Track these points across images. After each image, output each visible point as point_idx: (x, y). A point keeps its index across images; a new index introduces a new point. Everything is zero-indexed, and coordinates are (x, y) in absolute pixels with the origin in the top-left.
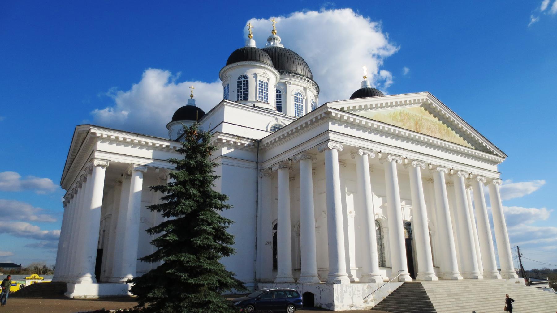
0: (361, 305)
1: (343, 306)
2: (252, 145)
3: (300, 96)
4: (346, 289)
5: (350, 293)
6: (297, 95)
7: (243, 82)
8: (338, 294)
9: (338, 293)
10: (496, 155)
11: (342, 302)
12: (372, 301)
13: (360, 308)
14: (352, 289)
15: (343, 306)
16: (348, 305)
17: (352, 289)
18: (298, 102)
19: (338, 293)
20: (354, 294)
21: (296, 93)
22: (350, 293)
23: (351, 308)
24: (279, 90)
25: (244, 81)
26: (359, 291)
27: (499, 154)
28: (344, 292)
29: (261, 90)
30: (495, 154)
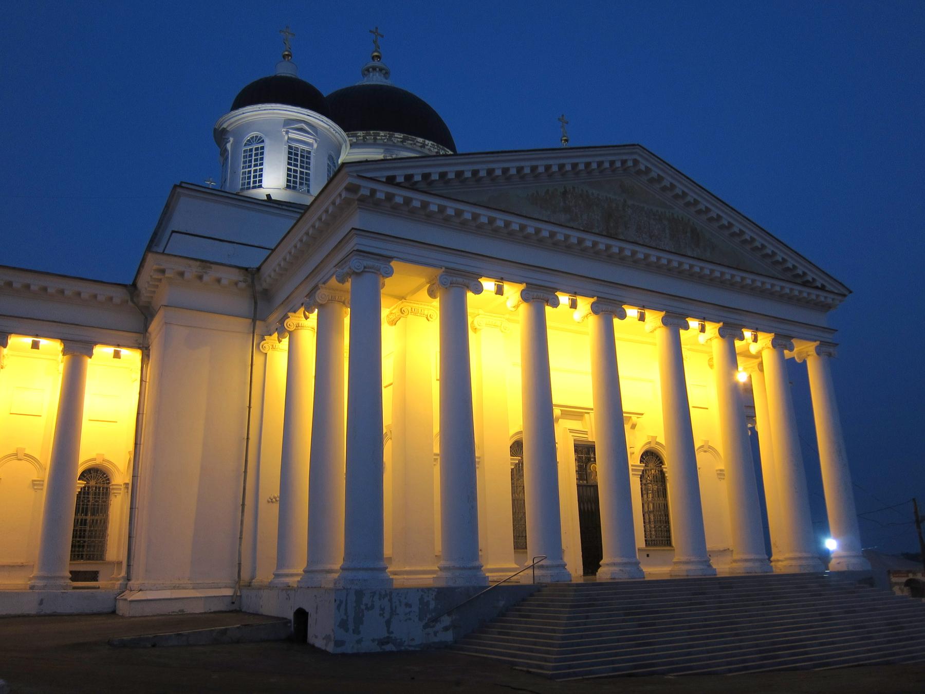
0: (413, 640)
1: (359, 642)
2: (240, 281)
4: (373, 601)
5: (383, 609)
7: (254, 150)
8: (346, 613)
9: (346, 610)
10: (823, 288)
11: (356, 631)
12: (446, 629)
13: (410, 646)
14: (390, 600)
15: (359, 642)
16: (373, 640)
17: (390, 600)
19: (346, 610)
20: (393, 612)
22: (383, 609)
23: (383, 647)
25: (257, 149)
26: (408, 605)
27: (829, 287)
28: (363, 607)
30: (820, 286)
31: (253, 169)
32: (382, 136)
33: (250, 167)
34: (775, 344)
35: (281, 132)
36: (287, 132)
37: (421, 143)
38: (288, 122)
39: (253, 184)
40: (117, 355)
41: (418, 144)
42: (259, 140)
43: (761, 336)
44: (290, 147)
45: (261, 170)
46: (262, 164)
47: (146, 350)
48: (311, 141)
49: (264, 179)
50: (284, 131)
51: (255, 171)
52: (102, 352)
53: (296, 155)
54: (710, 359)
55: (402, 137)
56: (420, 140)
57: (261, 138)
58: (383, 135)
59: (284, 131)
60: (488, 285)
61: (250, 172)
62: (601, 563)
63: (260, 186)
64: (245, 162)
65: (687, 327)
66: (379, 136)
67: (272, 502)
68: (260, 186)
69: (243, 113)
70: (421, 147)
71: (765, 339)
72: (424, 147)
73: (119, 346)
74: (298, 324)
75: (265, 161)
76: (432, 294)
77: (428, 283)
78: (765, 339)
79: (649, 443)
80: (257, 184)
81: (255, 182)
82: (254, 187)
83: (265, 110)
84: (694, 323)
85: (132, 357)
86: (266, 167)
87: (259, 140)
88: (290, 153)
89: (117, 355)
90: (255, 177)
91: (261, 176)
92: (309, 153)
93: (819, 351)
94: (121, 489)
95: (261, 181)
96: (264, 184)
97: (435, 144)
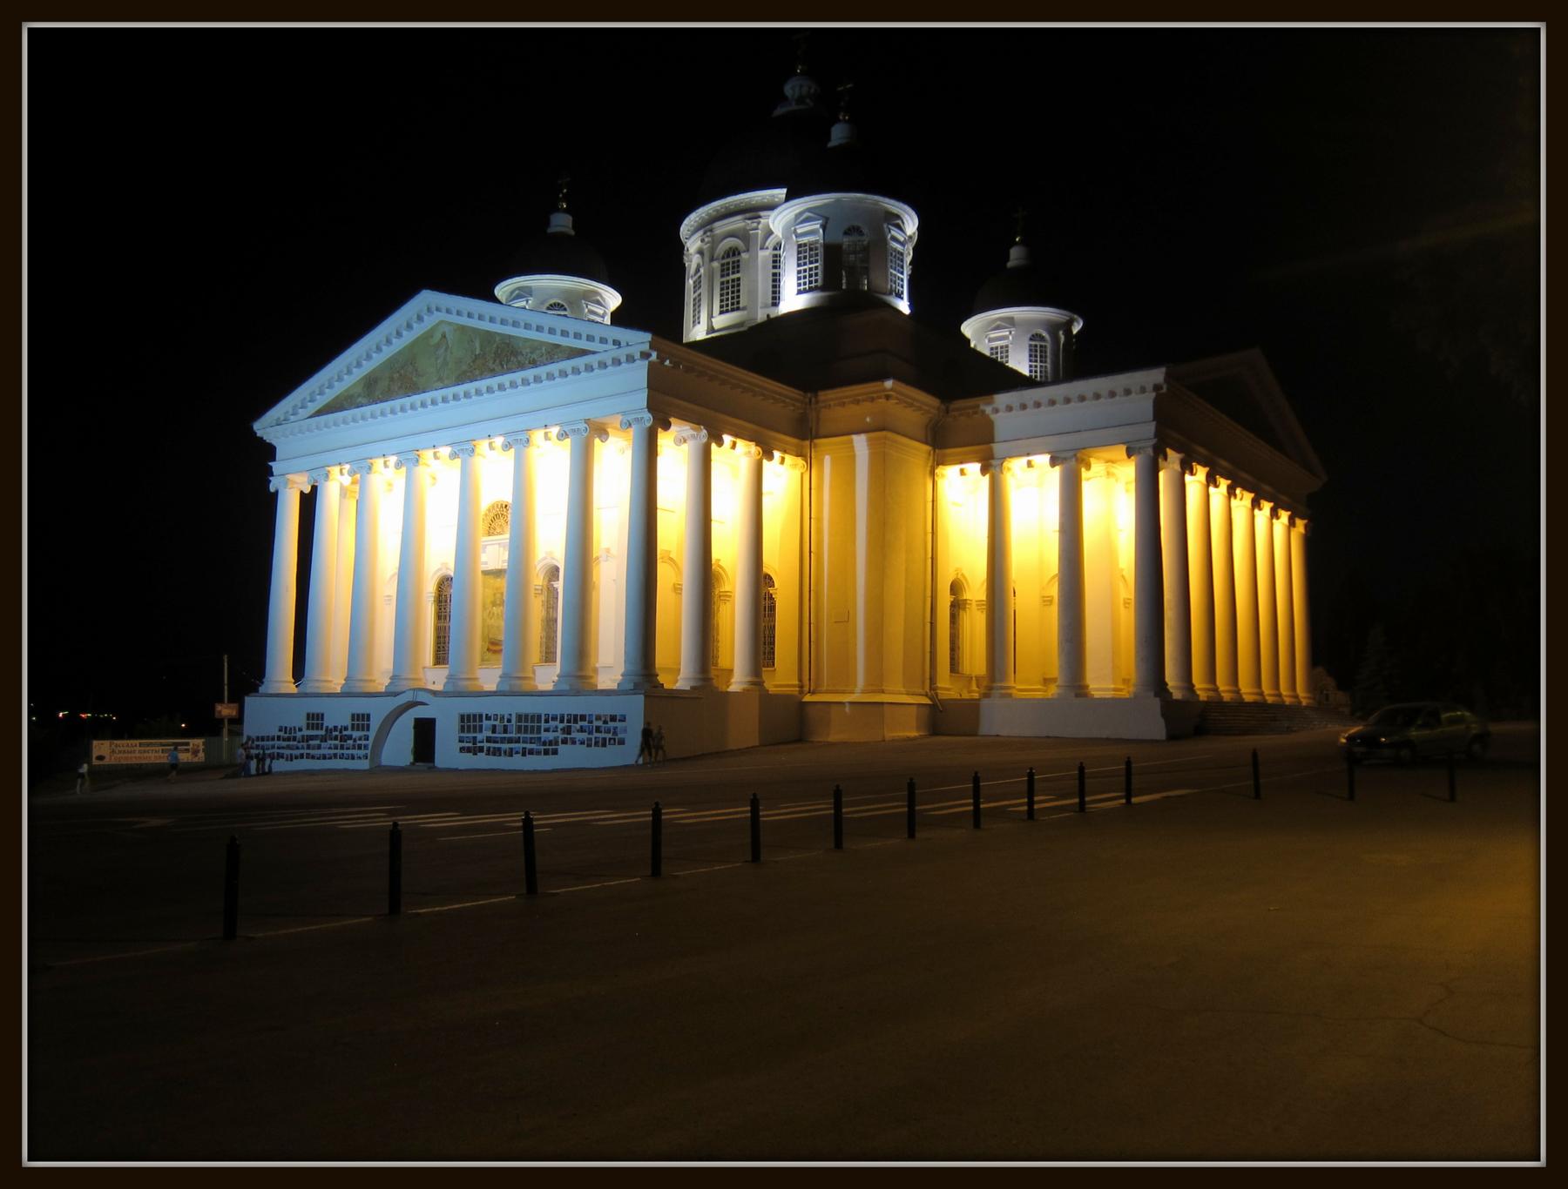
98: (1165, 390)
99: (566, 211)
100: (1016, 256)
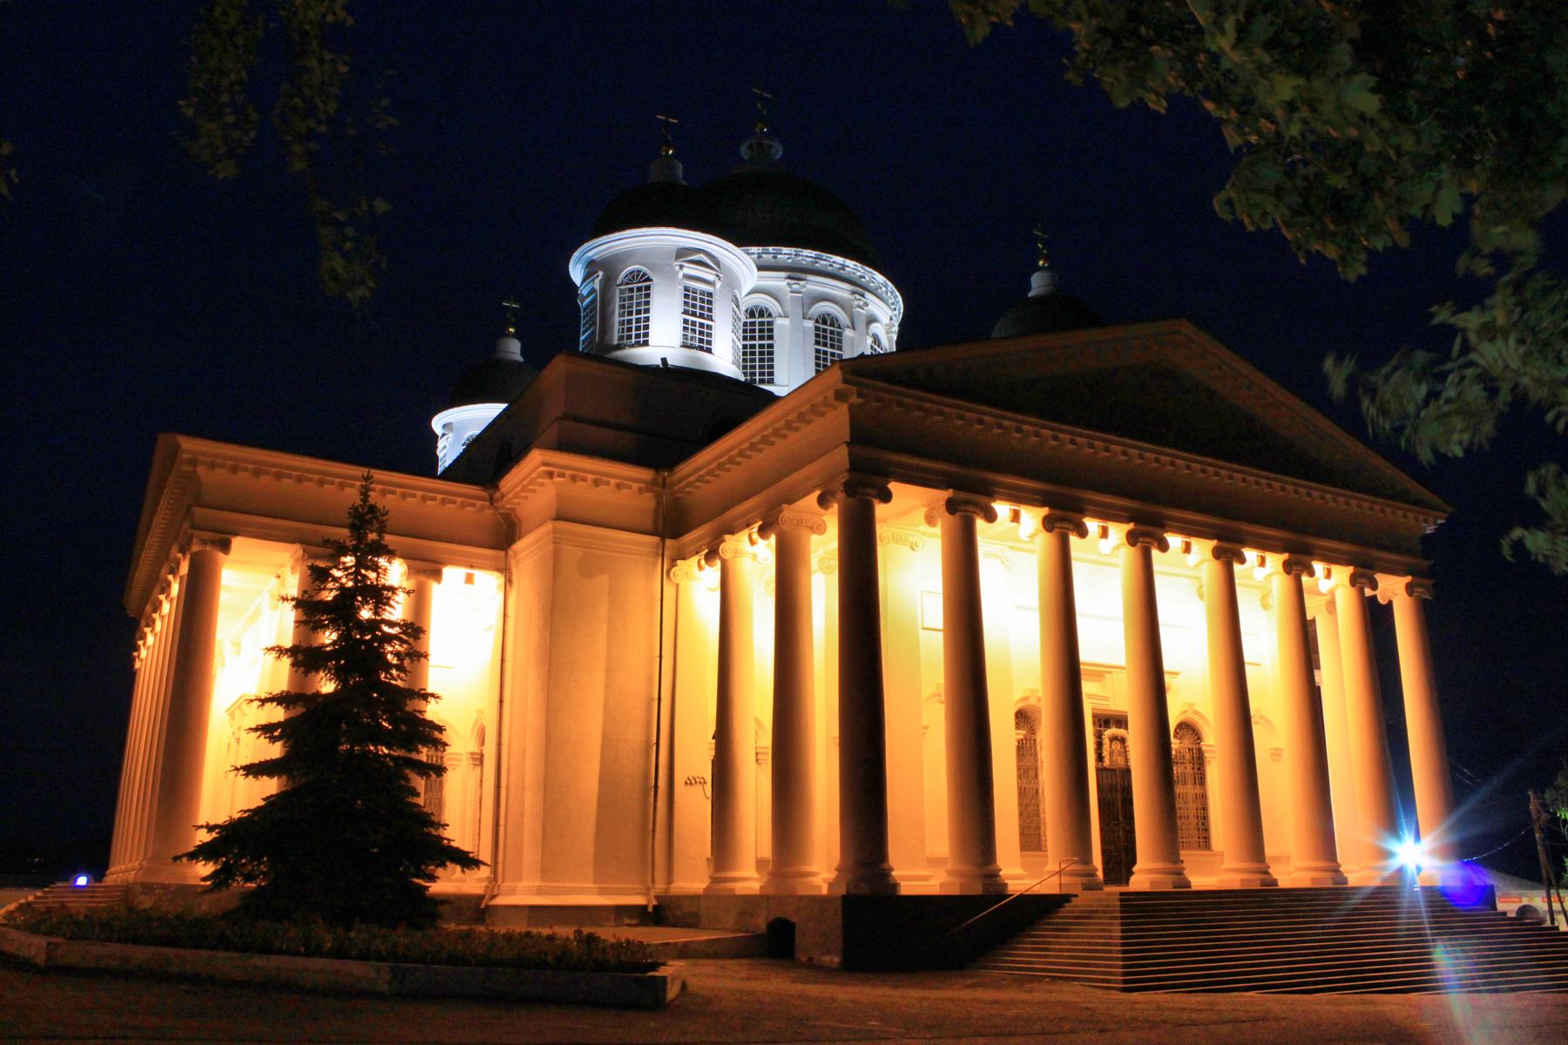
3: (832, 325)
6: (825, 322)
18: (825, 345)
21: (819, 316)
24: (767, 310)
25: (639, 289)
29: (706, 306)
31: (634, 317)
32: (785, 254)
33: (630, 313)
34: (1354, 580)
35: (671, 266)
36: (681, 267)
37: (840, 264)
38: (682, 253)
39: (636, 338)
40: (469, 579)
41: (835, 265)
42: (638, 276)
43: (1335, 569)
44: (686, 289)
45: (647, 319)
46: (647, 311)
47: (505, 570)
48: (710, 277)
49: (651, 331)
50: (677, 265)
51: (638, 320)
52: (453, 574)
53: (695, 299)
54: (1264, 596)
55: (813, 255)
56: (839, 260)
57: (644, 275)
58: (787, 252)
59: (677, 265)
60: (1002, 508)
61: (630, 322)
62: (1134, 869)
63: (646, 343)
64: (622, 307)
65: (1242, 560)
66: (781, 254)
67: (691, 784)
68: (646, 343)
69: (620, 239)
70: (840, 269)
71: (1342, 574)
72: (844, 270)
73: (472, 567)
74: (736, 550)
75: (652, 307)
76: (930, 521)
77: (924, 506)
78: (1342, 574)
79: (1185, 712)
80: (642, 339)
81: (638, 336)
82: (638, 344)
83: (651, 235)
84: (1251, 554)
85: (489, 582)
86: (653, 315)
87: (638, 276)
88: (686, 296)
89: (469, 579)
90: (638, 328)
91: (647, 327)
92: (710, 295)
93: (1410, 588)
94: (460, 760)
95: (646, 335)
96: (651, 339)
97: (859, 265)
98: (854, 399)
99: (514, 336)
100: (1038, 284)
